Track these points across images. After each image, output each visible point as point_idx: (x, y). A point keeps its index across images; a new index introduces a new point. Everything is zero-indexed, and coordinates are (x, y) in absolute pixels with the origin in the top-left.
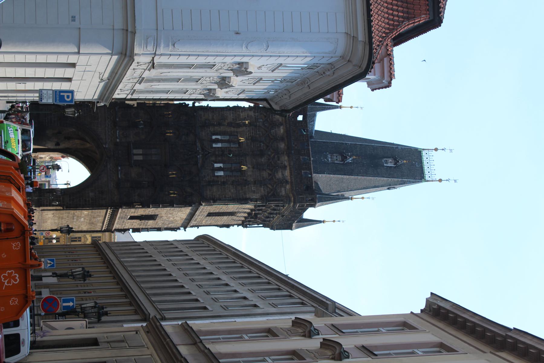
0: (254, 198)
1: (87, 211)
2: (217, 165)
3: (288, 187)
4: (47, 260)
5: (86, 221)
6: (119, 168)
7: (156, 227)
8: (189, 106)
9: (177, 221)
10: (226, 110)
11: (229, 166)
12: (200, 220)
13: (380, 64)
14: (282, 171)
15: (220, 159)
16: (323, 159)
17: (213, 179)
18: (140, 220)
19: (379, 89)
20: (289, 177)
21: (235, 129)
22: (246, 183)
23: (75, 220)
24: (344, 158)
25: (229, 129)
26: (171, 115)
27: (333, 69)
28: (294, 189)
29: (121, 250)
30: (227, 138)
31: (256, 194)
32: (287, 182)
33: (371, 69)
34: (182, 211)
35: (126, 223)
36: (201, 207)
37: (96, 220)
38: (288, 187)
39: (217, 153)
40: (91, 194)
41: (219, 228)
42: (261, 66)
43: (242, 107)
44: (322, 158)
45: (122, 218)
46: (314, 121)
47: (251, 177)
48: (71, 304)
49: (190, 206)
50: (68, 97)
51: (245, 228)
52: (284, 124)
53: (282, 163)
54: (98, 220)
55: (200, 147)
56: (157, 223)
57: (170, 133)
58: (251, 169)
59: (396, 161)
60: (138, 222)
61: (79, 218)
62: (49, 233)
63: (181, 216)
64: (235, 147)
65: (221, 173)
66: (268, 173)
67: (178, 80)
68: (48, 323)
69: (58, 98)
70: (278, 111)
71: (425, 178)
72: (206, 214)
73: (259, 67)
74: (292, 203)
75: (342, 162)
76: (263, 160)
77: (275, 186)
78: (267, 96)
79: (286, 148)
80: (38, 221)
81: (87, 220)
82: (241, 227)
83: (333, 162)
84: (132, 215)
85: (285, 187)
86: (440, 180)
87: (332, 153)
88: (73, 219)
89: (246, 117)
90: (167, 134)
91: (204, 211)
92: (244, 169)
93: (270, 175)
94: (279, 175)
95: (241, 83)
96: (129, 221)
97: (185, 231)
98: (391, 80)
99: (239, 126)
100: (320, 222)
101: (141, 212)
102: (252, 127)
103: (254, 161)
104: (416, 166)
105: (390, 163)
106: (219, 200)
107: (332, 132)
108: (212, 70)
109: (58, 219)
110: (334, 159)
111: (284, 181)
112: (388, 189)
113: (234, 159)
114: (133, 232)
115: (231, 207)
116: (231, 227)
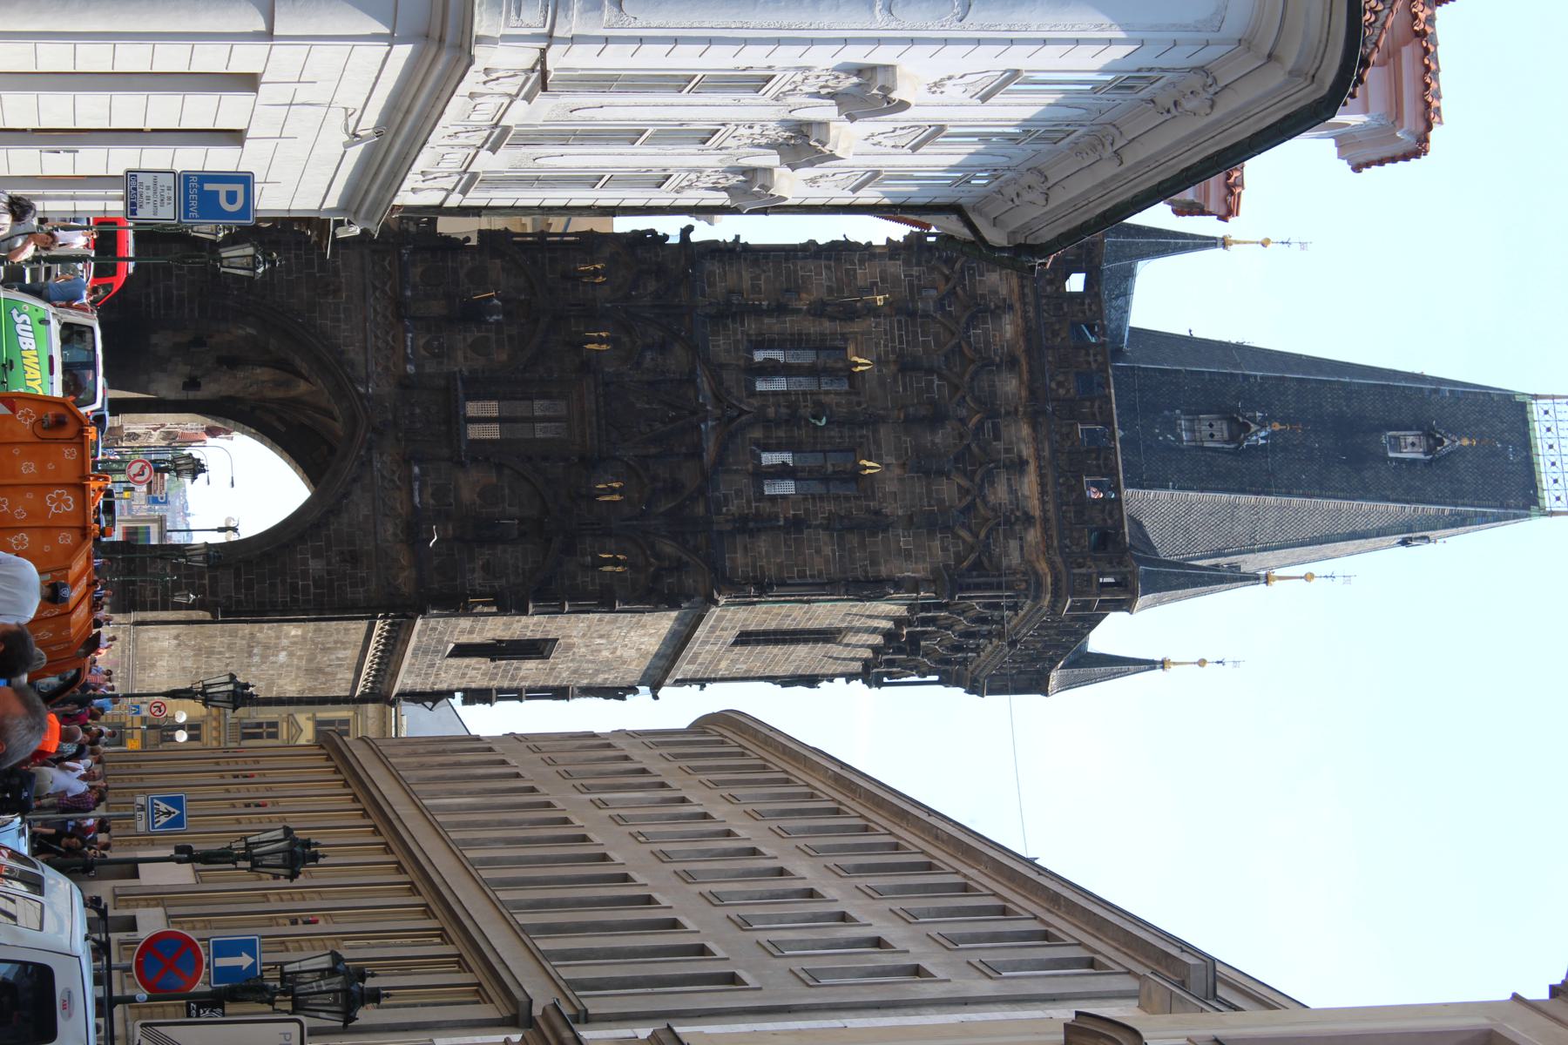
0: (909, 577)
1: (299, 627)
2: (770, 459)
3: (1033, 536)
4: (156, 801)
5: (295, 661)
6: (416, 470)
7: (551, 683)
9: (624, 663)
10: (805, 258)
11: (812, 460)
12: (709, 657)
13: (1386, 67)
14: (1009, 479)
15: (781, 434)
16: (1159, 434)
17: (756, 507)
18: (493, 660)
19: (1381, 162)
21: (838, 327)
22: (878, 524)
23: (256, 659)
24: (1240, 429)
25: (812, 327)
27: (1212, 90)
28: (1055, 543)
29: (422, 766)
30: (806, 357)
31: (916, 563)
32: (1028, 520)
33: (1355, 86)
34: (644, 626)
35: (440, 668)
36: (715, 611)
37: (332, 660)
38: (1033, 536)
39: (771, 412)
40: (315, 566)
41: (779, 686)
42: (942, 80)
44: (1157, 431)
45: (425, 652)
46: (1126, 294)
47: (896, 501)
48: (245, 961)
49: (673, 605)
50: (231, 197)
51: (875, 690)
52: (1017, 306)
53: (1008, 451)
54: (338, 659)
55: (709, 393)
56: (552, 669)
57: (601, 341)
58: (897, 471)
59: (1431, 442)
60: (483, 667)
61: (270, 652)
62: (163, 708)
63: (642, 643)
64: (837, 393)
65: (787, 488)
66: (959, 485)
67: (632, 136)
68: (159, 1029)
69: (194, 204)
70: (1002, 249)
71: (1540, 501)
72: (730, 636)
73: (935, 84)
74: (1048, 597)
75: (1232, 446)
76: (941, 438)
77: (982, 535)
78: (961, 194)
79: (1024, 393)
80: (123, 663)
81: (300, 658)
82: (858, 684)
83: (1199, 444)
84: (464, 639)
85: (1021, 539)
87: (1193, 413)
88: (250, 655)
89: (875, 284)
90: (589, 346)
91: (723, 624)
92: (868, 471)
93: (963, 492)
94: (1000, 493)
95: (867, 147)
96: (452, 661)
97: (656, 697)
98: (1429, 127)
99: (850, 314)
100: (1150, 665)
101: (495, 628)
103: (905, 442)
104: (1507, 458)
105: (1409, 449)
106: (778, 585)
107: (1196, 334)
108: (759, 98)
109: (195, 655)
110: (1200, 432)
111: (1018, 514)
112: (1404, 543)
113: (832, 433)
114: (465, 702)
115: (825, 613)
116: (824, 685)
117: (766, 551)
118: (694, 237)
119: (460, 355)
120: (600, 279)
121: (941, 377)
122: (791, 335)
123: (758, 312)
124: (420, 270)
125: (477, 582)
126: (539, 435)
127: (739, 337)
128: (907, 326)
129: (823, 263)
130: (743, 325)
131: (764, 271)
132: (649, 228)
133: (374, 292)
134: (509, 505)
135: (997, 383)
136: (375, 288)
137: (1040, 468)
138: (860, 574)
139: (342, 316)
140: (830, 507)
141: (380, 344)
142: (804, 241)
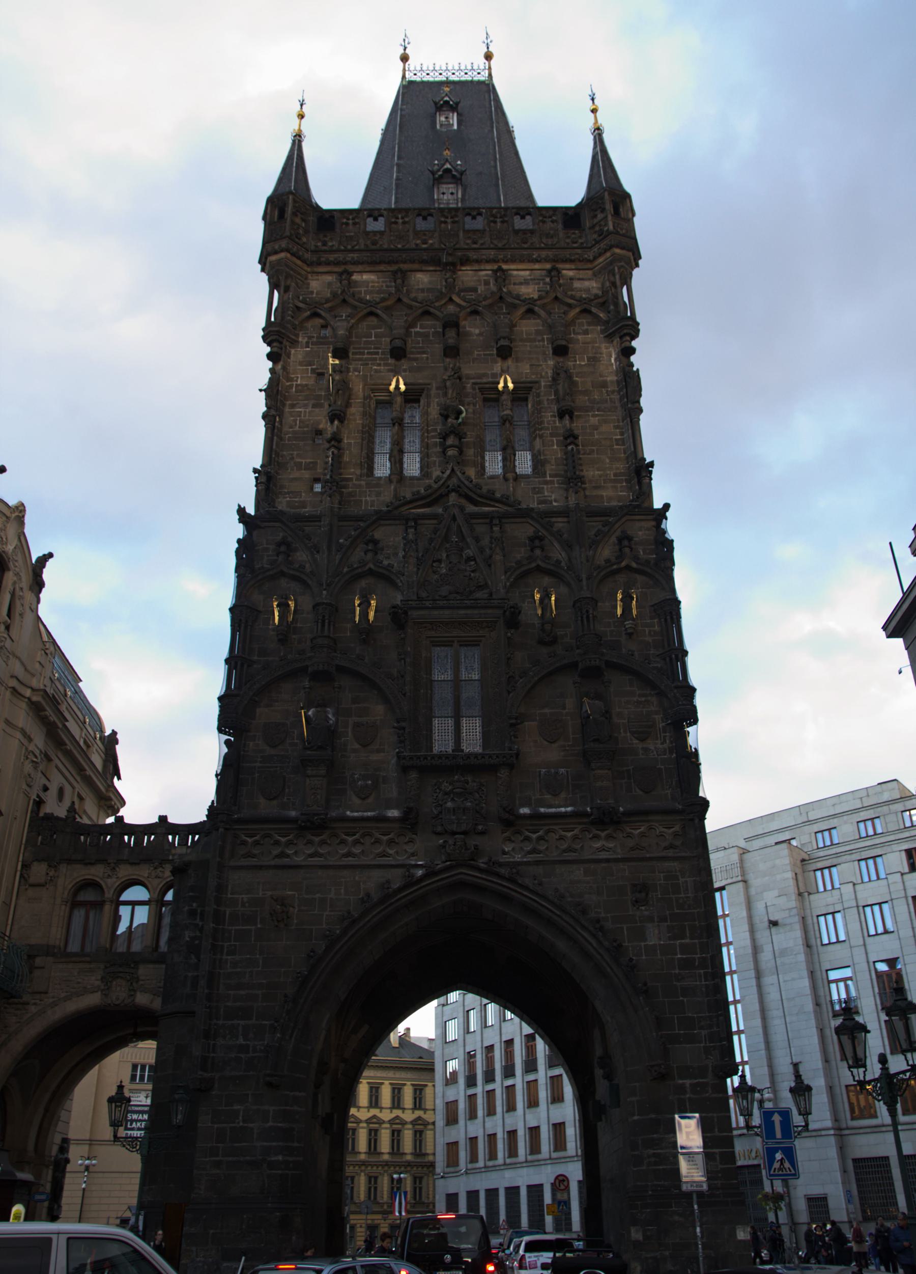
3: (571, 273)
6: (525, 811)
10: (281, 422)
11: (492, 436)
14: (514, 284)
20: (537, 266)
26: (287, 598)
31: (601, 354)
32: (554, 273)
40: (654, 936)
43: (268, 375)
47: (541, 365)
53: (487, 283)
57: (365, 605)
58: (510, 362)
59: (445, 109)
76: (474, 329)
83: (460, 200)
85: (571, 279)
86: (488, 57)
89: (312, 369)
94: (530, 291)
99: (343, 388)
103: (478, 355)
113: (470, 410)
117: (598, 470)
118: (251, 510)
119: (375, 757)
120: (292, 604)
121: (412, 325)
122: (363, 440)
124: (262, 801)
125: (661, 746)
126: (476, 676)
128: (360, 348)
129: (287, 410)
130: (351, 479)
131: (292, 458)
132: (234, 554)
133: (288, 856)
134: (564, 708)
135: (421, 286)
136: (282, 855)
138: (616, 397)
139: (318, 895)
140: (549, 416)
141: (357, 850)
142: (263, 423)
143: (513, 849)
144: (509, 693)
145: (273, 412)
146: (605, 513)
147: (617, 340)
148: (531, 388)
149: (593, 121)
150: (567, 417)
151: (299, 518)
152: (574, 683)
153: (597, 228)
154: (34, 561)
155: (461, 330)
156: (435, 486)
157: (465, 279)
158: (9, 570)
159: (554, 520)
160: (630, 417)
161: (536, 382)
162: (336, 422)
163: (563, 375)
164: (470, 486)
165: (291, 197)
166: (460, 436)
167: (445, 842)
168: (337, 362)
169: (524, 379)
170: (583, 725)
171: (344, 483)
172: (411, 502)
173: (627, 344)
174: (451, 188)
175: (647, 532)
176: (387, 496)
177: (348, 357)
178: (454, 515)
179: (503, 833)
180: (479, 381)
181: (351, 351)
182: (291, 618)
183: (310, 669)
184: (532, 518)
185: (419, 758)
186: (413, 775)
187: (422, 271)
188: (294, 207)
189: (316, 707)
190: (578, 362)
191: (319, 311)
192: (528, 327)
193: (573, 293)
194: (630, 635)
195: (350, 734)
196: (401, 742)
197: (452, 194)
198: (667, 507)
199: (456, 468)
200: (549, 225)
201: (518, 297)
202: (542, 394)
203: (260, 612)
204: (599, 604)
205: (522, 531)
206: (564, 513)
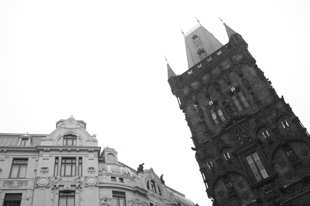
3: (235, 57)
6: (285, 186)
8: (196, 152)
14: (224, 67)
15: (233, 109)
17: (253, 104)
20: (227, 60)
22: (244, 81)
32: (231, 59)
53: (218, 70)
57: (227, 155)
76: (221, 82)
86: (198, 21)
93: (230, 71)
94: (228, 66)
99: (201, 111)
102: (199, 102)
117: (263, 97)
118: (194, 147)
119: (245, 189)
120: (211, 163)
123: (206, 127)
127: (214, 128)
137: (220, 63)
138: (258, 78)
140: (246, 91)
142: (188, 126)
143: (287, 197)
144: (267, 160)
145: (189, 123)
146: (269, 106)
147: (252, 65)
148: (239, 87)
149: (222, 22)
150: (250, 89)
151: (204, 144)
152: (282, 150)
153: (234, 44)
154: (160, 178)
155: (218, 84)
156: (229, 121)
157: (214, 72)
158: (155, 182)
159: (259, 114)
160: (264, 80)
161: (239, 85)
162: (202, 118)
163: (244, 81)
164: (236, 116)
165: (172, 78)
166: (229, 107)
167: (270, 203)
168: (196, 105)
169: (237, 86)
170: (289, 159)
171: (210, 131)
172: (225, 127)
173: (254, 65)
174: (203, 54)
175: (282, 105)
176: (220, 128)
177: (198, 103)
178: (236, 125)
179: (283, 194)
180: (227, 92)
181: (198, 101)
182: (212, 166)
183: (221, 176)
184: (254, 116)
185: (254, 185)
186: (255, 190)
187: (204, 76)
188: (173, 79)
189: (227, 183)
190: (246, 75)
191: (188, 97)
192: (232, 74)
193: (237, 61)
194: (290, 131)
195: (237, 186)
196: (248, 183)
197: (204, 55)
198: (282, 96)
199: (231, 114)
200: (225, 51)
201: (226, 69)
202: (242, 87)
203: (206, 168)
204: (278, 128)
205: (252, 121)
206: (260, 111)
